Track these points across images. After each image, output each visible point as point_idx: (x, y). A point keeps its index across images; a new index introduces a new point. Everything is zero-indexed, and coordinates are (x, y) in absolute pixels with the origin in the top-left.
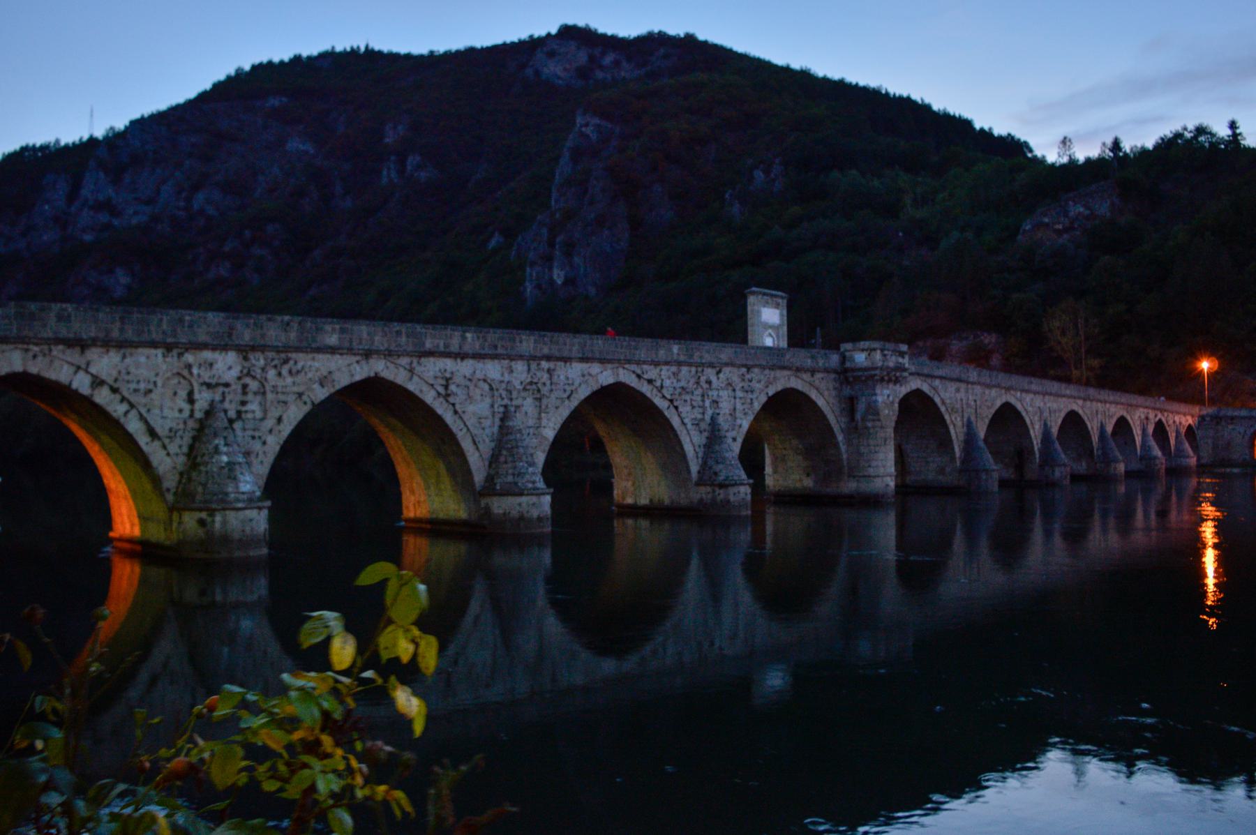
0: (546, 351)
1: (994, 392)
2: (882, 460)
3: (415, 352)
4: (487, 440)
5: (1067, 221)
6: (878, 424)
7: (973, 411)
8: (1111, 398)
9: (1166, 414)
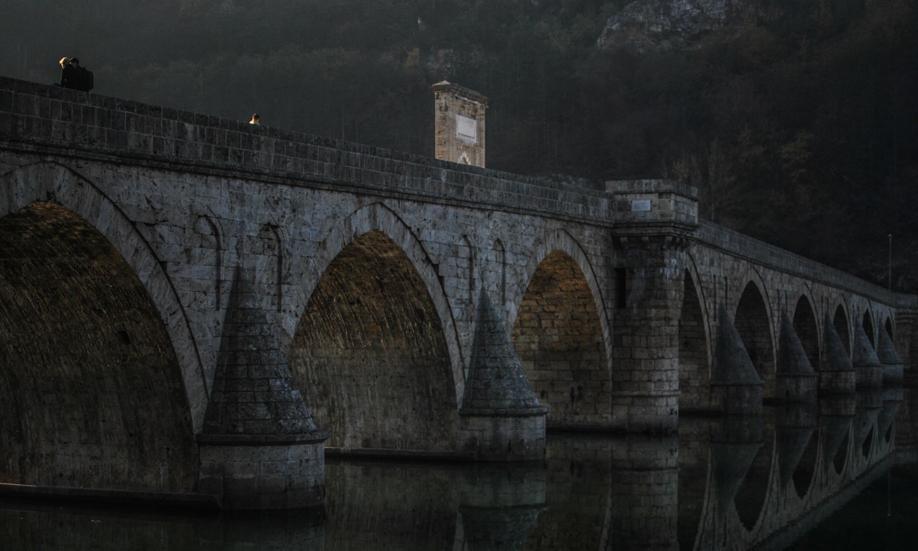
0: (290, 167)
1: (743, 265)
2: (666, 371)
3: (114, 154)
4: (209, 336)
5: (667, 22)
6: (662, 312)
7: (724, 296)
8: (832, 279)
9: (872, 302)
